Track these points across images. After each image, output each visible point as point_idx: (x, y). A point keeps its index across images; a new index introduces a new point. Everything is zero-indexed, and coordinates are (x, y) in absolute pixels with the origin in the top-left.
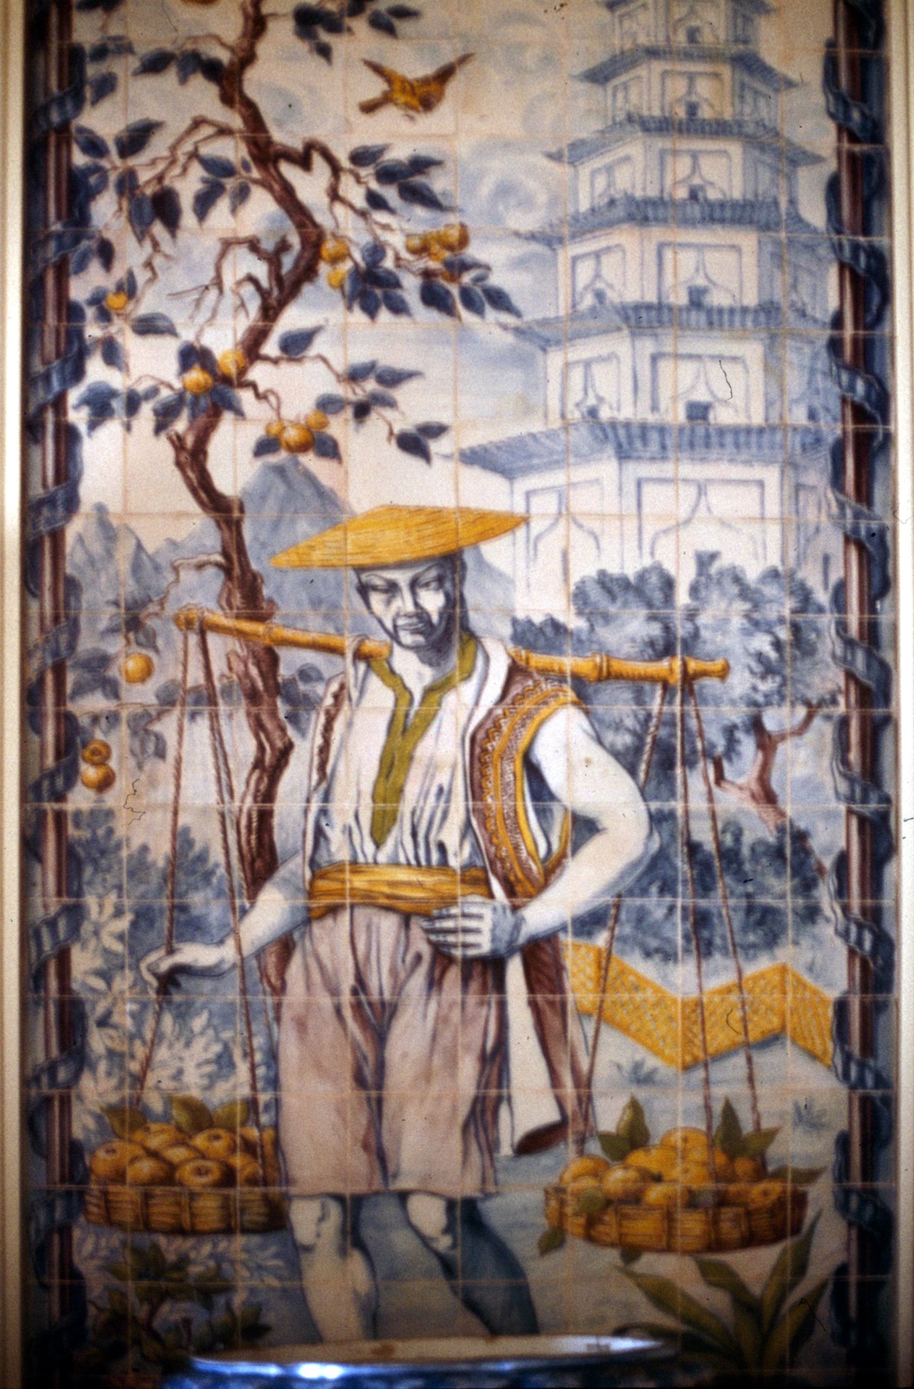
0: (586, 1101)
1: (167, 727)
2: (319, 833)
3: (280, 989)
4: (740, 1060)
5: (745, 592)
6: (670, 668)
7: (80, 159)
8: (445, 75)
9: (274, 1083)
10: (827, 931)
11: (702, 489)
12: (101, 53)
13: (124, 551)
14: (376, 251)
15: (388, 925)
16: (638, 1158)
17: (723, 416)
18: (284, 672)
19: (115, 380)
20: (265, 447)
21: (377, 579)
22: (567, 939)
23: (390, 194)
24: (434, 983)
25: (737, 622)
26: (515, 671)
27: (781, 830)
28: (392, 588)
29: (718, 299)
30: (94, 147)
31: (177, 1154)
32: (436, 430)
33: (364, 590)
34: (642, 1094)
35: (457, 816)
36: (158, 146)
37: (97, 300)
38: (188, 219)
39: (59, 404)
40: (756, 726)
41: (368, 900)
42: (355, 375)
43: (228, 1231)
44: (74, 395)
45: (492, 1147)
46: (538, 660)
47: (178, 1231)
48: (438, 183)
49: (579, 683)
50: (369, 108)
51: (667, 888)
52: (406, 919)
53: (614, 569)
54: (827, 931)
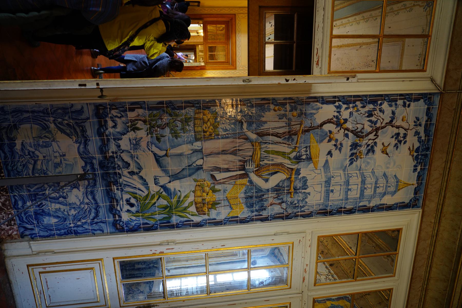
0: (220, 183)
1: (284, 119)
2: (266, 143)
3: (239, 138)
4: (228, 204)
5: (304, 199)
6: (292, 190)
7: (379, 102)
8: (387, 154)
9: (223, 138)
10: (250, 214)
11: (320, 192)
12: (396, 105)
13: (314, 111)
14: (360, 146)
15: (251, 154)
16: (211, 191)
17: (331, 194)
18: (293, 137)
19: (342, 110)
20: (330, 132)
21: (308, 149)
22: (248, 179)
23: (369, 147)
24: (240, 161)
25: (299, 198)
26: (292, 169)
27: (266, 207)
28: (306, 151)
29: (349, 192)
30: (381, 104)
31: (209, 124)
32: (331, 156)
33: (306, 147)
34: (222, 191)
35: (268, 162)
36: (381, 114)
37: (356, 106)
38: (368, 119)
39: (339, 101)
40: (283, 202)
41: (255, 150)
42: (341, 144)
43: (195, 132)
44: (341, 103)
45: (212, 171)
46: (294, 172)
47: (194, 124)
48: (370, 154)
49: (290, 178)
50: (383, 144)
51: (256, 192)
52: (252, 156)
53: (308, 182)
54: (250, 214)
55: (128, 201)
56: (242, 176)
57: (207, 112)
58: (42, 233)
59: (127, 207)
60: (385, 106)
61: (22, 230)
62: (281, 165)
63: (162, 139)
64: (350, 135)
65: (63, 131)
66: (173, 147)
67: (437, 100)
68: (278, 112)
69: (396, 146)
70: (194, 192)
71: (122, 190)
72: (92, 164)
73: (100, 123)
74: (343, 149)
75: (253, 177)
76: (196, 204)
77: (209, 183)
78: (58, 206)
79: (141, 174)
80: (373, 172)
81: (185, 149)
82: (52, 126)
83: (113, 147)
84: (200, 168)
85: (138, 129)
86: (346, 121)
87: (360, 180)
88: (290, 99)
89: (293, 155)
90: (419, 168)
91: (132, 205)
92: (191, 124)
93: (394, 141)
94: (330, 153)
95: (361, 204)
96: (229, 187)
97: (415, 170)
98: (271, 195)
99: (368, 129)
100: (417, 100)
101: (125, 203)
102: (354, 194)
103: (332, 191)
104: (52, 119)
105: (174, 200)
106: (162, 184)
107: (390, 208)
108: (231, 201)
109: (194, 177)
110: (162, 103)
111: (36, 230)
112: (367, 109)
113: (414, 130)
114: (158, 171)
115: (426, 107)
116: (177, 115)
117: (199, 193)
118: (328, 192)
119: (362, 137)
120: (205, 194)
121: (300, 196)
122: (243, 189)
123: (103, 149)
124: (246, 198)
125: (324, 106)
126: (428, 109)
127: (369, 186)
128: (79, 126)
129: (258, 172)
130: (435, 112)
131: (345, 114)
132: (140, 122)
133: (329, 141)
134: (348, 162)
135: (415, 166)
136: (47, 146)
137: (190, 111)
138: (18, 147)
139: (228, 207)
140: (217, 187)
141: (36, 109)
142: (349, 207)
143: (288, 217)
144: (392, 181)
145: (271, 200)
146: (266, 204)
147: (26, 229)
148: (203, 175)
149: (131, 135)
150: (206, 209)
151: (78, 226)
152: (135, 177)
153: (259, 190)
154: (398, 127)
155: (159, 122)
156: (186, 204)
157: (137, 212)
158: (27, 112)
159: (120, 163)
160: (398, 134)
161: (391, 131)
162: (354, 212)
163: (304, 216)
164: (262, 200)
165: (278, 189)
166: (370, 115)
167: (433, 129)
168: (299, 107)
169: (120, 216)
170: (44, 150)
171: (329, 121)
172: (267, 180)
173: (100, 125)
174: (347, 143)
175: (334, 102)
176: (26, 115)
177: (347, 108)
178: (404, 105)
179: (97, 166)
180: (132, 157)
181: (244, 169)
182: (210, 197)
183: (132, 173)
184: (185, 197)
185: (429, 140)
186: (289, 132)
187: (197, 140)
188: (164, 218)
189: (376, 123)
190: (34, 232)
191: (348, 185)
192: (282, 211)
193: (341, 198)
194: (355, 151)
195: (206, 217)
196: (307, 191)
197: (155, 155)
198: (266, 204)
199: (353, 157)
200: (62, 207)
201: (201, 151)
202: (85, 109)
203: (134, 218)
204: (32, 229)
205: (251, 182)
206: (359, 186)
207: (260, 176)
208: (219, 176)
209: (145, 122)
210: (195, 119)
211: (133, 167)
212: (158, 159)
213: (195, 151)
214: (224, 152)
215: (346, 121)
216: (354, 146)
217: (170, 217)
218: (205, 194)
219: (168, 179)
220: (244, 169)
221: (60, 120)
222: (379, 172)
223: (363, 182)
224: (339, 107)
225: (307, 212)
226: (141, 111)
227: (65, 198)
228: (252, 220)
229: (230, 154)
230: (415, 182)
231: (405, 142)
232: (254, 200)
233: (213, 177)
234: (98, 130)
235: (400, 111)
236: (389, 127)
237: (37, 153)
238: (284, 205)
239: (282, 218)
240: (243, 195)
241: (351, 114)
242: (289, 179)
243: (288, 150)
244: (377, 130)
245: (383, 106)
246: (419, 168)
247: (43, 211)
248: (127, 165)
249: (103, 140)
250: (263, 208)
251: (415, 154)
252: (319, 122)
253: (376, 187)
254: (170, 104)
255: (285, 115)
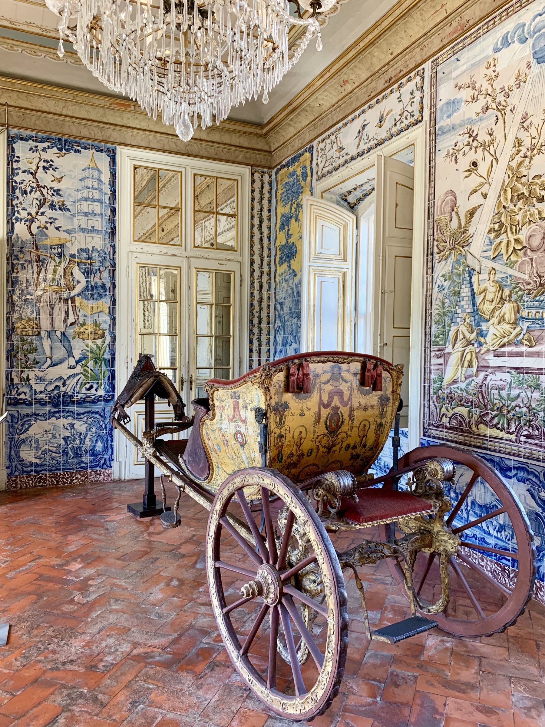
0: (78, 319)
1: (26, 265)
5: (98, 252)
6: (89, 261)
7: (14, 184)
8: (62, 178)
9: (39, 315)
12: (17, 169)
13: (20, 240)
14: (53, 201)
15: (54, 294)
17: (95, 228)
19: (19, 216)
20: (39, 227)
23: (55, 194)
26: (70, 260)
29: (95, 212)
30: (16, 183)
31: (26, 325)
32: (61, 227)
33: (51, 248)
36: (25, 183)
37: (16, 204)
38: (29, 194)
39: (11, 219)
40: (99, 270)
42: (50, 218)
44: (13, 218)
45: (67, 325)
47: (26, 335)
48: (60, 192)
49: (78, 263)
50: (52, 181)
55: (87, 390)
56: (73, 302)
57: (16, 325)
58: (110, 453)
59: (93, 390)
60: (17, 179)
61: (105, 466)
62: (65, 270)
63: (37, 360)
64: (42, 210)
65: (27, 430)
66: (44, 353)
67: (13, 131)
68: (20, 270)
69: (55, 169)
70: (84, 340)
71: (78, 393)
72: (55, 412)
73: (21, 403)
74: (55, 217)
75: (73, 294)
76: (94, 339)
77: (77, 327)
78: (87, 439)
79: (66, 378)
80: (78, 190)
81: (46, 343)
82: (22, 436)
83: (42, 396)
84: (63, 334)
85: (28, 377)
86: (29, 214)
87: (84, 202)
88: (8, 260)
89: (58, 260)
90: (77, 148)
91: (91, 387)
92: (25, 338)
93: (51, 171)
94: (58, 228)
95: (107, 202)
96: (81, 313)
97: (79, 152)
98: (92, 279)
99: (38, 195)
100: (13, 149)
101: (89, 392)
102: (97, 208)
103: (93, 227)
104: (17, 436)
105: (90, 355)
106: (75, 364)
107: (114, 175)
108: (95, 312)
109: (71, 339)
110: (7, 359)
111: (106, 456)
112: (20, 195)
113: (41, 153)
114: (64, 365)
115: (20, 141)
116: (18, 348)
117: (85, 336)
118: (93, 230)
119: (45, 200)
120: (87, 332)
121: (95, 255)
122: (85, 301)
123: (43, 404)
124: (93, 299)
125: (15, 232)
126: (22, 139)
127: (91, 194)
128: (23, 418)
129: (70, 289)
130: (25, 133)
131: (23, 214)
132: (22, 375)
133: (47, 228)
134: (67, 213)
135: (75, 151)
136: (37, 441)
137: (15, 337)
138: (38, 461)
139: (100, 314)
140: (81, 321)
141: (9, 446)
142: (109, 213)
143: (114, 266)
144: (87, 173)
145: (97, 279)
146: (99, 284)
147: (104, 463)
148: (70, 332)
149: (32, 382)
150: (100, 332)
151: (106, 427)
152: (67, 382)
153: (87, 288)
154: (38, 168)
155: (23, 361)
156: (94, 346)
157: (98, 383)
158: (10, 452)
159: (55, 392)
160: (44, 168)
161: (40, 174)
162: (115, 208)
163: (114, 252)
164: (96, 287)
165: (87, 273)
166: (25, 192)
167: (41, 135)
168: (15, 253)
169: (101, 396)
170: (41, 444)
171: (29, 228)
172: (78, 282)
173: (24, 403)
174: (50, 213)
175: (12, 223)
176: (13, 453)
177: (18, 213)
178: (17, 161)
179: (57, 409)
180: (51, 383)
181: (67, 300)
182: (90, 327)
183: (64, 385)
184: (87, 346)
185: (51, 139)
186: (37, 262)
187: (39, 334)
188: (105, 364)
189: (33, 188)
190: (108, 458)
191: (88, 213)
192: (107, 271)
193: (100, 220)
194: (57, 207)
195: (107, 332)
196: (91, 249)
197: (50, 366)
198: (99, 284)
199: (63, 208)
200: (89, 436)
201: (49, 332)
202: (11, 413)
203: (103, 386)
204: (105, 459)
205: (78, 295)
206: (90, 203)
207: (74, 287)
208: (71, 319)
209: (22, 372)
210: (22, 334)
211: (60, 383)
212: (53, 365)
213: (49, 336)
214: (51, 314)
215: (29, 214)
216: (52, 206)
217: (105, 359)
218: (87, 332)
219: (71, 358)
220: (67, 300)
221: (18, 431)
222: (79, 185)
223: (87, 199)
224: (17, 220)
225: (110, 249)
226: (14, 374)
227: (81, 434)
228: (114, 295)
229: (53, 309)
230: (91, 151)
231: (52, 161)
232: (95, 292)
233: (72, 324)
234: (27, 405)
235: (23, 165)
236: (37, 176)
237: (43, 449)
238: (102, 269)
239: (114, 271)
240: (90, 301)
241: (23, 209)
242: (78, 264)
243: (53, 263)
244: (39, 186)
245: (18, 181)
246: (77, 148)
247: (91, 450)
248: (57, 387)
249: (35, 403)
250: (104, 286)
251: (64, 151)
252: (29, 237)
253: (93, 188)
254: (8, 352)
255: (22, 265)
